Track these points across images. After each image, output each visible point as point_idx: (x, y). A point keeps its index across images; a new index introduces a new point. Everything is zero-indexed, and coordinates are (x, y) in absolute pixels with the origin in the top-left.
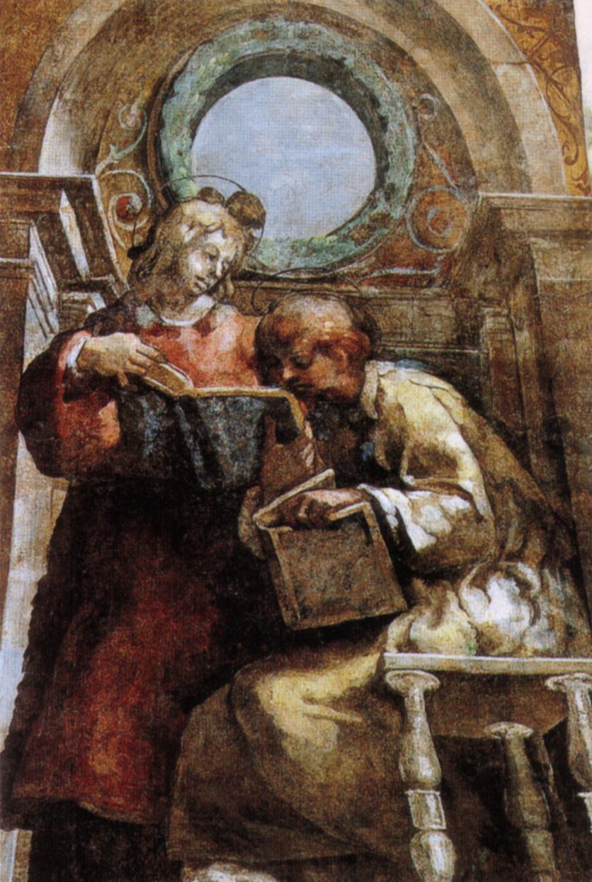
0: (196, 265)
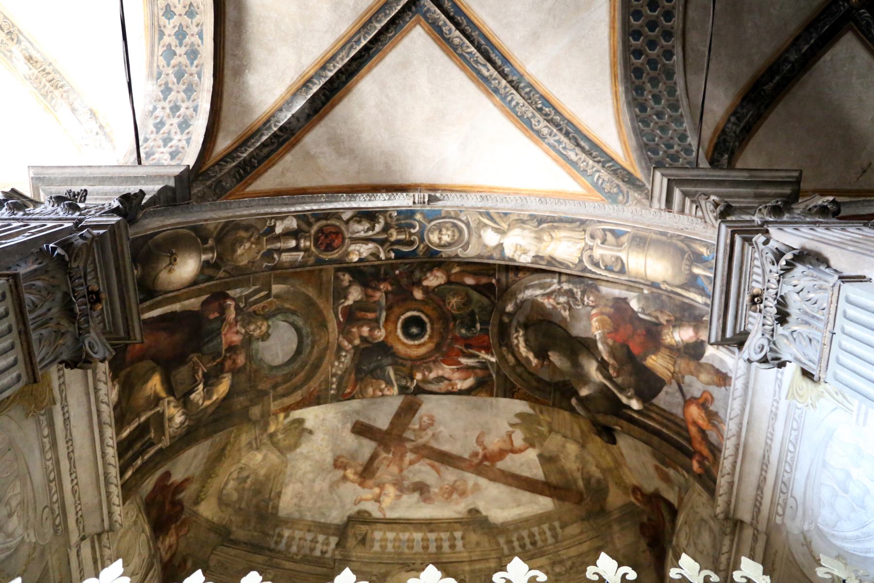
0: (252, 327)
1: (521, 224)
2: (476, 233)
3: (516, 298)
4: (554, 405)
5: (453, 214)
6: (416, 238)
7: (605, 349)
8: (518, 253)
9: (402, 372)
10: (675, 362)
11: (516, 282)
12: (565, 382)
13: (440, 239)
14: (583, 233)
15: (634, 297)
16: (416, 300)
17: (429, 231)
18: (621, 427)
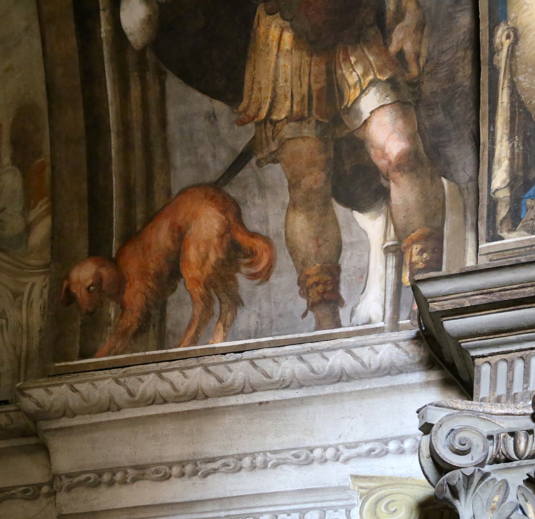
10: (300, 119)
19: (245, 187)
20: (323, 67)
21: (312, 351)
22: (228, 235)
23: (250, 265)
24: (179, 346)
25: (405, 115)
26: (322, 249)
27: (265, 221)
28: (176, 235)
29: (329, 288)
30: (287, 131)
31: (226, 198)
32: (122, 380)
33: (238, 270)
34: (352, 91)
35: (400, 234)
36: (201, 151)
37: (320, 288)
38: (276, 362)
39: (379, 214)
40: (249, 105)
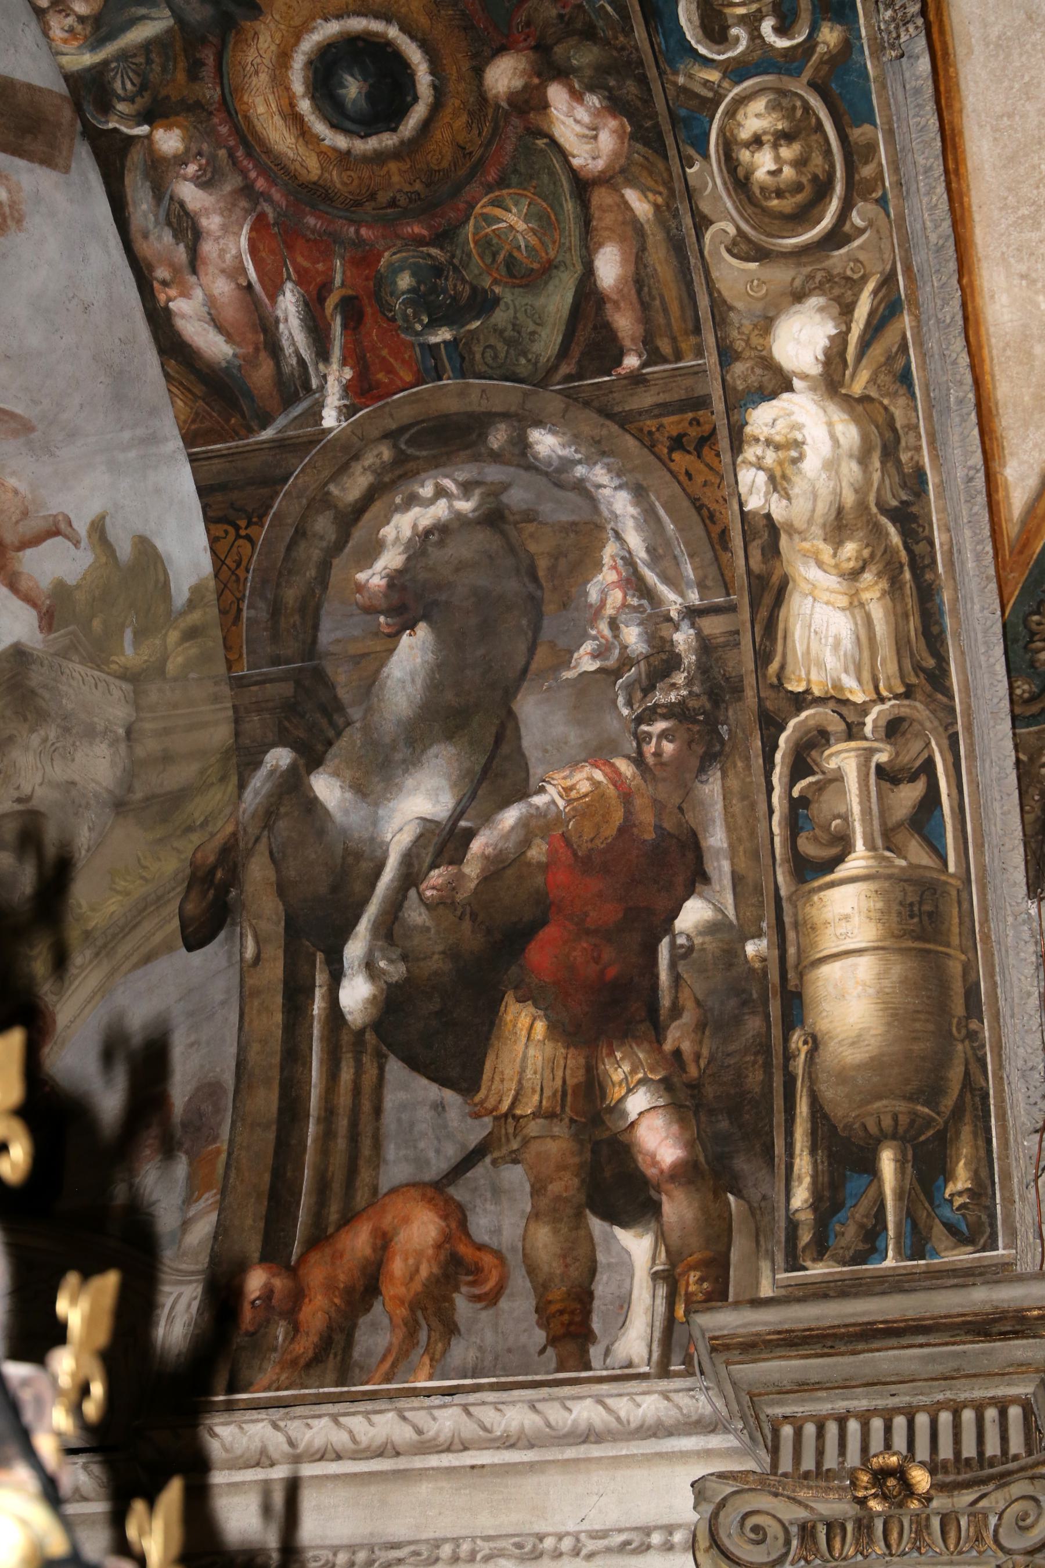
1: (877, 441)
2: (810, 277)
3: (589, 461)
4: (239, 684)
5: (867, 171)
6: (741, 48)
7: (506, 837)
8: (770, 457)
9: (164, 69)
10: (551, 1116)
11: (651, 448)
12: (339, 707)
13: (757, 141)
14: (901, 690)
15: (718, 910)
16: (478, 72)
17: (782, 93)
18: (257, 959)
19: (476, 1189)
20: (582, 1061)
21: (551, 1399)
22: (447, 1246)
23: (473, 1284)
24: (366, 1383)
25: (682, 1121)
26: (571, 1269)
27: (498, 1231)
28: (379, 1242)
29: (577, 1319)
30: (533, 1128)
31: (449, 1200)
32: (282, 1424)
33: (457, 1289)
34: (617, 1089)
35: (674, 1257)
36: (422, 1145)
37: (566, 1317)
38: (499, 1410)
39: (647, 1231)
40: (487, 1097)
